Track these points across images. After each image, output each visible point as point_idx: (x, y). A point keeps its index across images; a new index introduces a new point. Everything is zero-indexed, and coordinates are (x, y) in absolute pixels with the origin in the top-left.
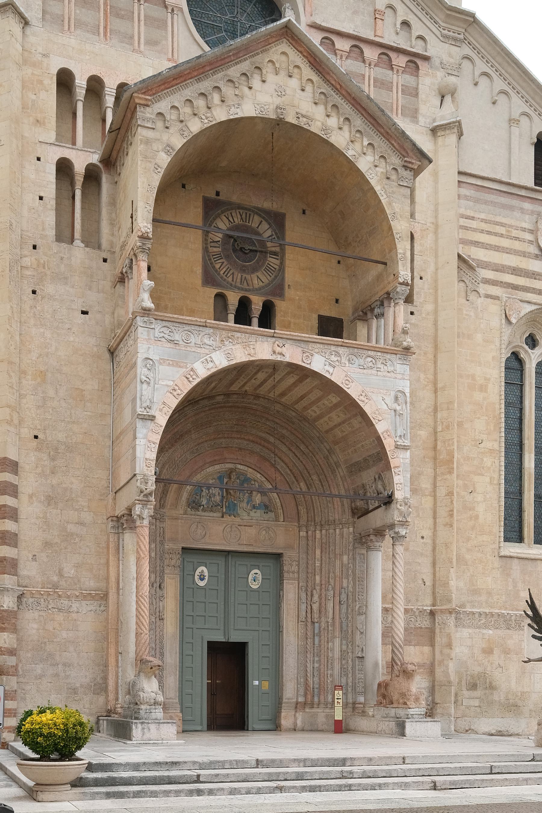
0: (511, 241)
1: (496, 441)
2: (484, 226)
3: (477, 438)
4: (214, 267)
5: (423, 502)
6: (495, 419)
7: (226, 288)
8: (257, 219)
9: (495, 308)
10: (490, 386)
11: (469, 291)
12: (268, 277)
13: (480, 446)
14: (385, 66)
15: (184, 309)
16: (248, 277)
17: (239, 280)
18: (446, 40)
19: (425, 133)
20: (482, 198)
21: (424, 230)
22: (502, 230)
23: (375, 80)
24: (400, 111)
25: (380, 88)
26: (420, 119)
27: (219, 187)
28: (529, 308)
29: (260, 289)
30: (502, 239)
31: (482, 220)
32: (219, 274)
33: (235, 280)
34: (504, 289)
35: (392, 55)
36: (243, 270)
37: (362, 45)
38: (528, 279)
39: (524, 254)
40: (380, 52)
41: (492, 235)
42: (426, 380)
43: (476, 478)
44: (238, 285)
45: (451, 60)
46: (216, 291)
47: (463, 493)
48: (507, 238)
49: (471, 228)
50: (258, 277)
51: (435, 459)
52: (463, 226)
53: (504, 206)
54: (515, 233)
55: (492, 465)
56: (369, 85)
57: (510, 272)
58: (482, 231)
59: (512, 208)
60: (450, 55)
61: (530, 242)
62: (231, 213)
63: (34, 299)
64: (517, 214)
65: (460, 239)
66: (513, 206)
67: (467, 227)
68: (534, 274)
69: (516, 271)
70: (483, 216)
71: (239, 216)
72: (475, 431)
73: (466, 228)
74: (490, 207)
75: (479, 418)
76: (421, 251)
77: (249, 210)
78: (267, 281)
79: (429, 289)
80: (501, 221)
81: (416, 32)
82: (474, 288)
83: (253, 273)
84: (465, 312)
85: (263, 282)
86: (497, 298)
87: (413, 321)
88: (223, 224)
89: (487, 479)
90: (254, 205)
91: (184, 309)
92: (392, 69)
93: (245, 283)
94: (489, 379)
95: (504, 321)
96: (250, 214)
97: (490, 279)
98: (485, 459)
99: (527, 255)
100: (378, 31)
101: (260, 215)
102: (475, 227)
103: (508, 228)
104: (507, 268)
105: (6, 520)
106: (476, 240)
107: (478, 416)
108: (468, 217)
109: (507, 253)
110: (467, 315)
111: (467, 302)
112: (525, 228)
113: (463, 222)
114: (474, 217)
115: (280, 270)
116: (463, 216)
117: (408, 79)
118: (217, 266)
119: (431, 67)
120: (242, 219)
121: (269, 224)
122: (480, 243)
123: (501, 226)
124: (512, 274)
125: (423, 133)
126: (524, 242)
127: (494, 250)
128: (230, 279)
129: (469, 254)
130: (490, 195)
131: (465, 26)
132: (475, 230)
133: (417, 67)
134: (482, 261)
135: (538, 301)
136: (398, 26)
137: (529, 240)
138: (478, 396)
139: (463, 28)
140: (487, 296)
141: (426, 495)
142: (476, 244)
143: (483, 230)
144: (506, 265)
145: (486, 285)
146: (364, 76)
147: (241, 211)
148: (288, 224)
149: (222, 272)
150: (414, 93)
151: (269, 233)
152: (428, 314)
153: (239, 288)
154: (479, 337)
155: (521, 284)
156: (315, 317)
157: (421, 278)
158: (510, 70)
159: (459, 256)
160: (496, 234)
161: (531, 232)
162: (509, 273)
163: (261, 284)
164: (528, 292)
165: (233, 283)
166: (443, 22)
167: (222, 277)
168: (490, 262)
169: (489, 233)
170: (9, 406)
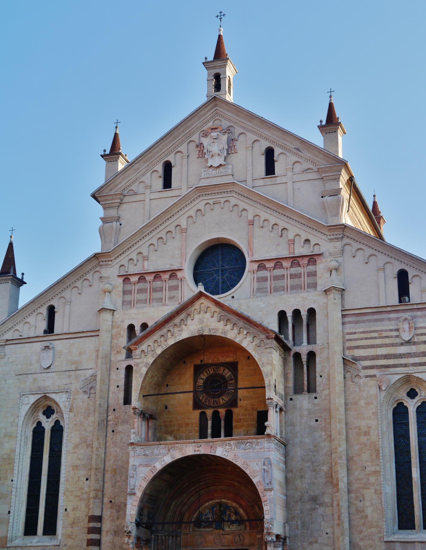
0: (382, 339)
1: (378, 465)
2: (363, 336)
3: (364, 465)
4: (199, 399)
5: (327, 511)
6: (377, 451)
7: (206, 409)
8: (222, 368)
9: (372, 382)
10: (372, 431)
11: (353, 377)
12: (229, 397)
13: (366, 470)
14: (297, 266)
15: (184, 424)
16: (217, 400)
17: (212, 403)
18: (332, 241)
19: (321, 294)
20: (360, 320)
21: (322, 349)
22: (376, 335)
23: (291, 275)
24: (306, 287)
25: (294, 278)
26: (318, 287)
27: (202, 358)
28: (397, 377)
29: (224, 404)
30: (376, 340)
31: (362, 332)
32: (201, 402)
33: (210, 403)
34: (378, 370)
35: (299, 260)
36: (214, 397)
37: (281, 261)
38: (396, 360)
39: (392, 345)
40: (292, 260)
41: (369, 339)
42: (326, 435)
43: (365, 491)
44: (212, 405)
45: (337, 250)
46: (200, 411)
47: (355, 502)
48: (379, 338)
49: (354, 339)
50: (223, 399)
51: (332, 482)
52: (348, 339)
53: (376, 320)
54: (385, 334)
55: (376, 481)
56: (287, 279)
57: (383, 358)
58: (362, 339)
59: (382, 320)
60: (335, 247)
61: (397, 336)
62: (208, 369)
63: (113, 435)
64: (386, 323)
65: (347, 347)
66: (383, 319)
67: (351, 339)
68: (401, 355)
69: (387, 357)
70: (361, 330)
71: (212, 370)
72: (362, 461)
73: (350, 340)
74: (366, 323)
75: (365, 453)
76: (320, 361)
77: (218, 365)
78: (228, 400)
79: (326, 382)
80: (375, 329)
81: (312, 243)
82: (356, 374)
83: (220, 397)
84: (352, 389)
85: (225, 401)
86: (375, 376)
87: (316, 402)
88: (204, 376)
89: (373, 491)
90: (220, 362)
91: (184, 424)
92: (300, 266)
93: (216, 404)
94: (371, 427)
95: (378, 390)
96: (218, 367)
97: (369, 366)
98: (370, 478)
99: (395, 345)
100: (291, 250)
101: (224, 366)
102: (356, 338)
103: (380, 332)
104: (380, 356)
105: (91, 547)
106: (358, 345)
107: (364, 451)
108: (351, 334)
109: (380, 347)
110: (353, 391)
111: (353, 383)
112: (392, 329)
113: (348, 337)
114: (356, 332)
115: (235, 392)
116: (348, 334)
117: (311, 268)
118: (201, 398)
119: (324, 258)
120: (214, 371)
121: (229, 369)
122: (361, 346)
123: (375, 332)
124: (384, 359)
125: (320, 295)
126: (392, 337)
127: (371, 348)
128: (207, 403)
129: (353, 355)
130: (366, 317)
131: (342, 230)
132: (356, 340)
133: (316, 261)
134: (362, 356)
135: (403, 372)
136: (302, 243)
137: (396, 336)
138: (363, 439)
139: (341, 231)
140: (367, 377)
141: (328, 506)
142: (358, 347)
143: (362, 338)
144: (379, 355)
145: (366, 370)
146: (284, 275)
147: (214, 367)
148: (240, 367)
149: (203, 401)
150: (313, 274)
151: (229, 373)
152: (326, 396)
153: (213, 407)
154: (362, 403)
155: (392, 364)
156: (255, 413)
157: (321, 376)
158: (373, 243)
159: (344, 359)
160: (371, 338)
161: (397, 330)
162: (382, 359)
163: (224, 402)
164: (397, 367)
165: (209, 405)
166: (328, 232)
167: (203, 403)
168: (368, 356)
169: (366, 339)
170: (94, 490)
